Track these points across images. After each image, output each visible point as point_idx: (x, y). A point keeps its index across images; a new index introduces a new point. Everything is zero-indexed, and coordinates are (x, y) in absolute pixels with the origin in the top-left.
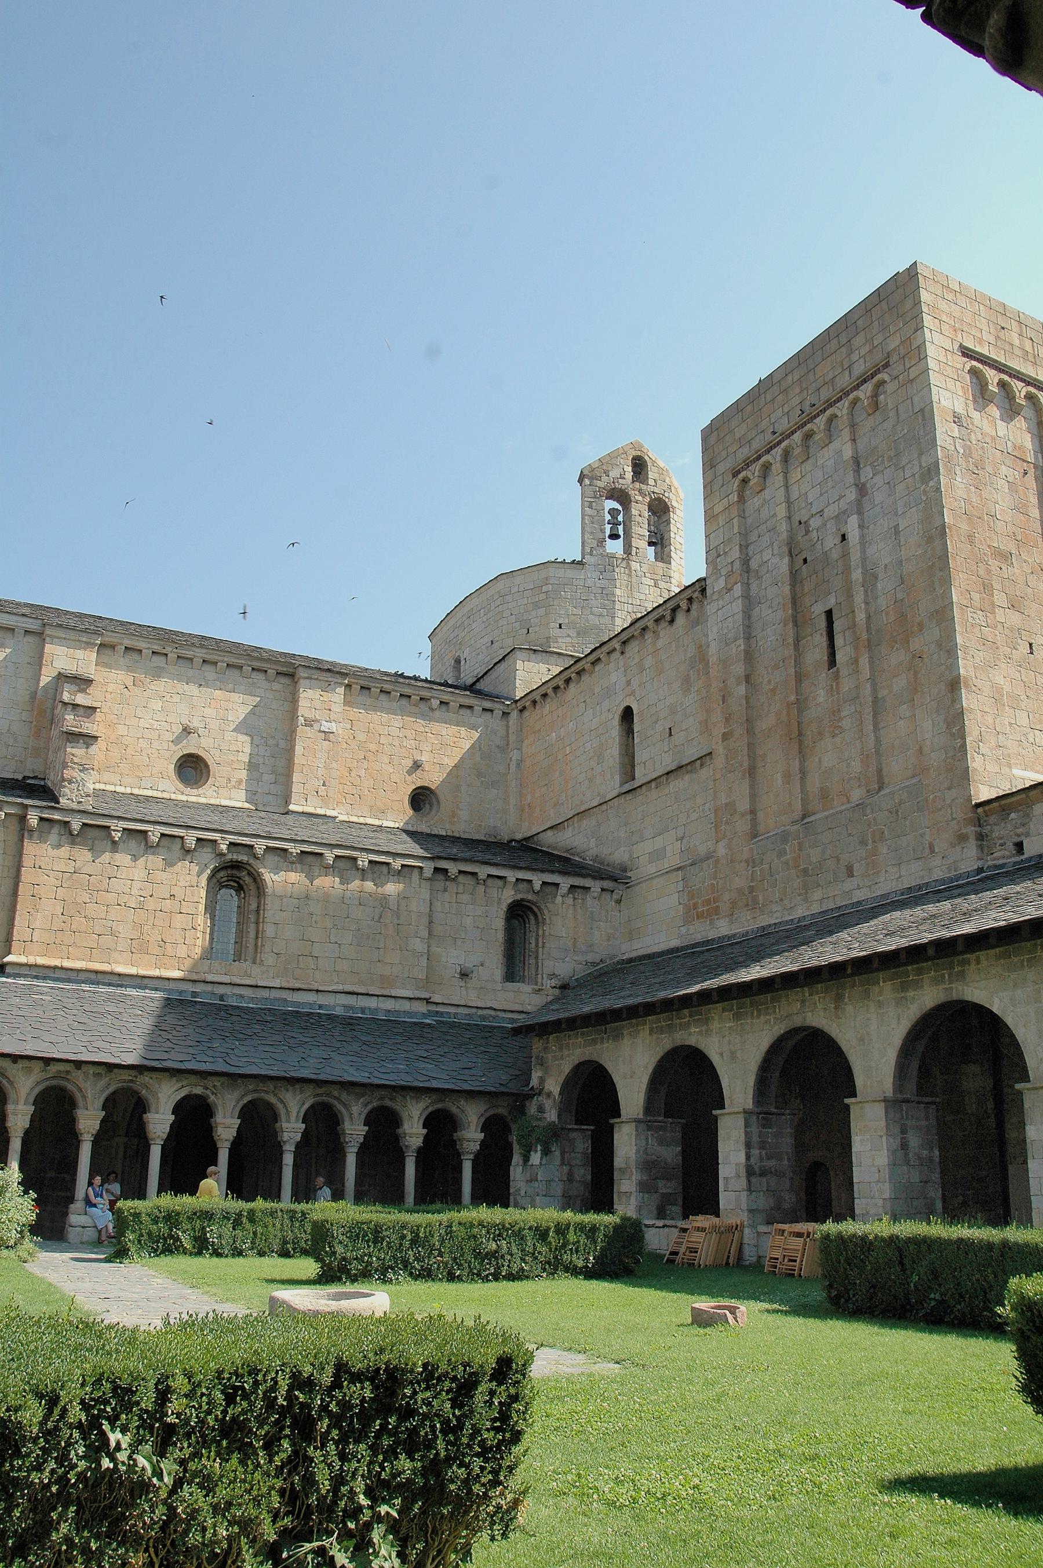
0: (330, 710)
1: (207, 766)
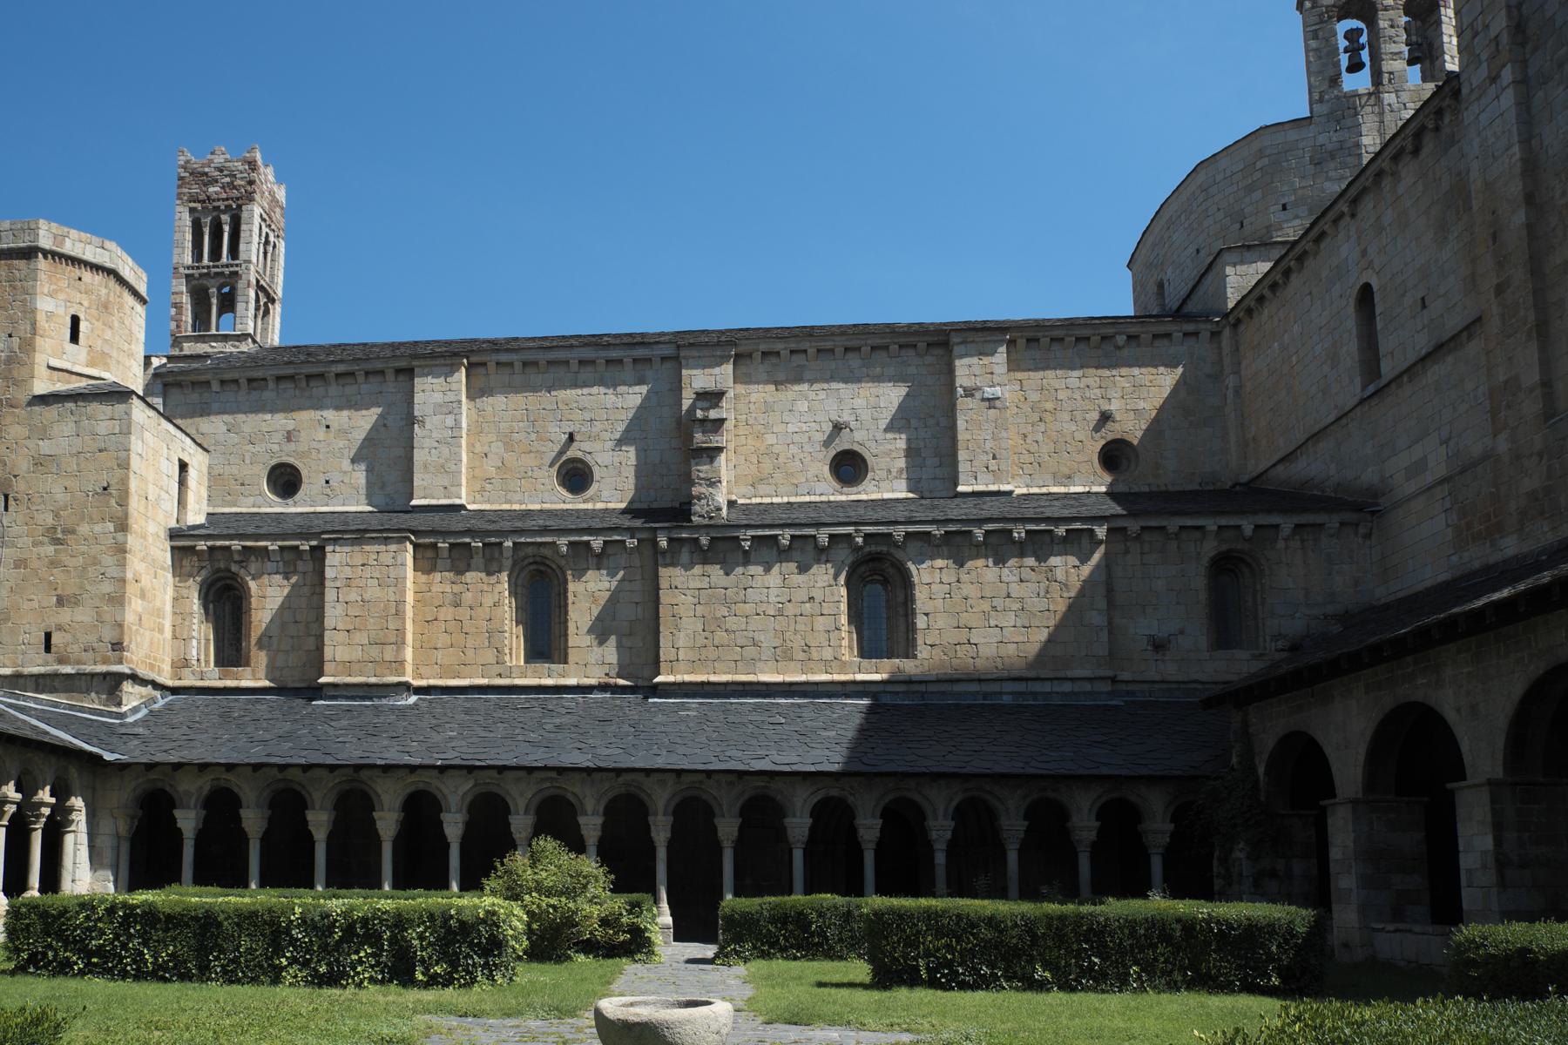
1: (864, 461)
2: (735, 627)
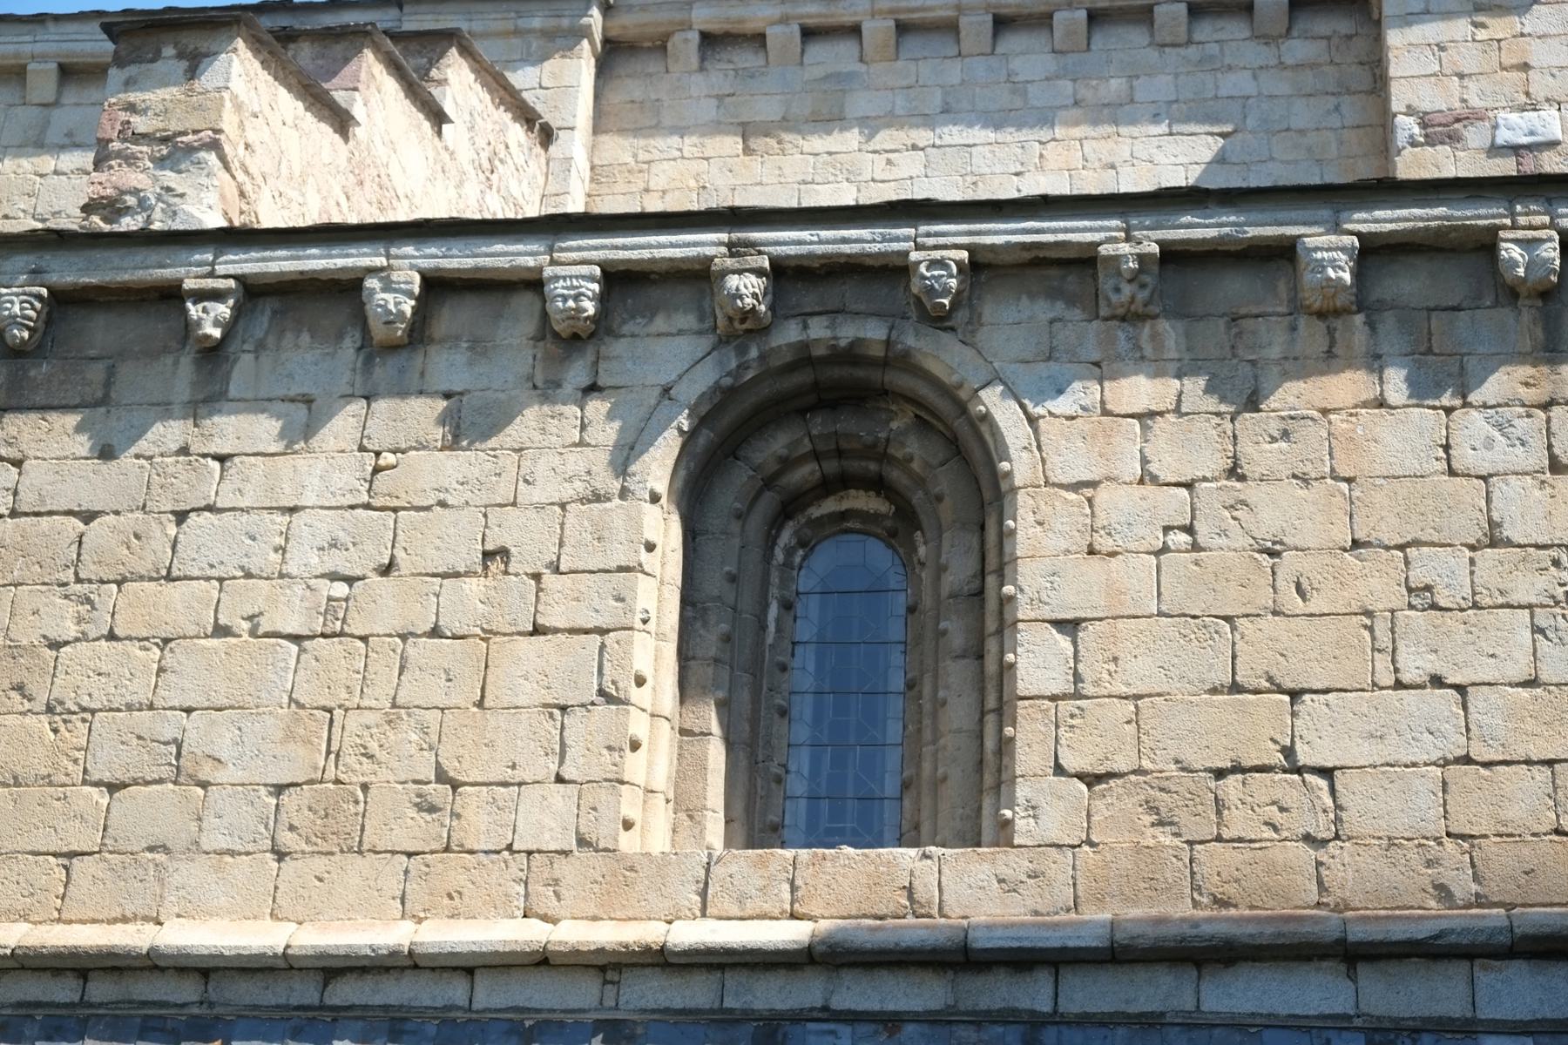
0: (1525, 67)
2: (96, 692)
